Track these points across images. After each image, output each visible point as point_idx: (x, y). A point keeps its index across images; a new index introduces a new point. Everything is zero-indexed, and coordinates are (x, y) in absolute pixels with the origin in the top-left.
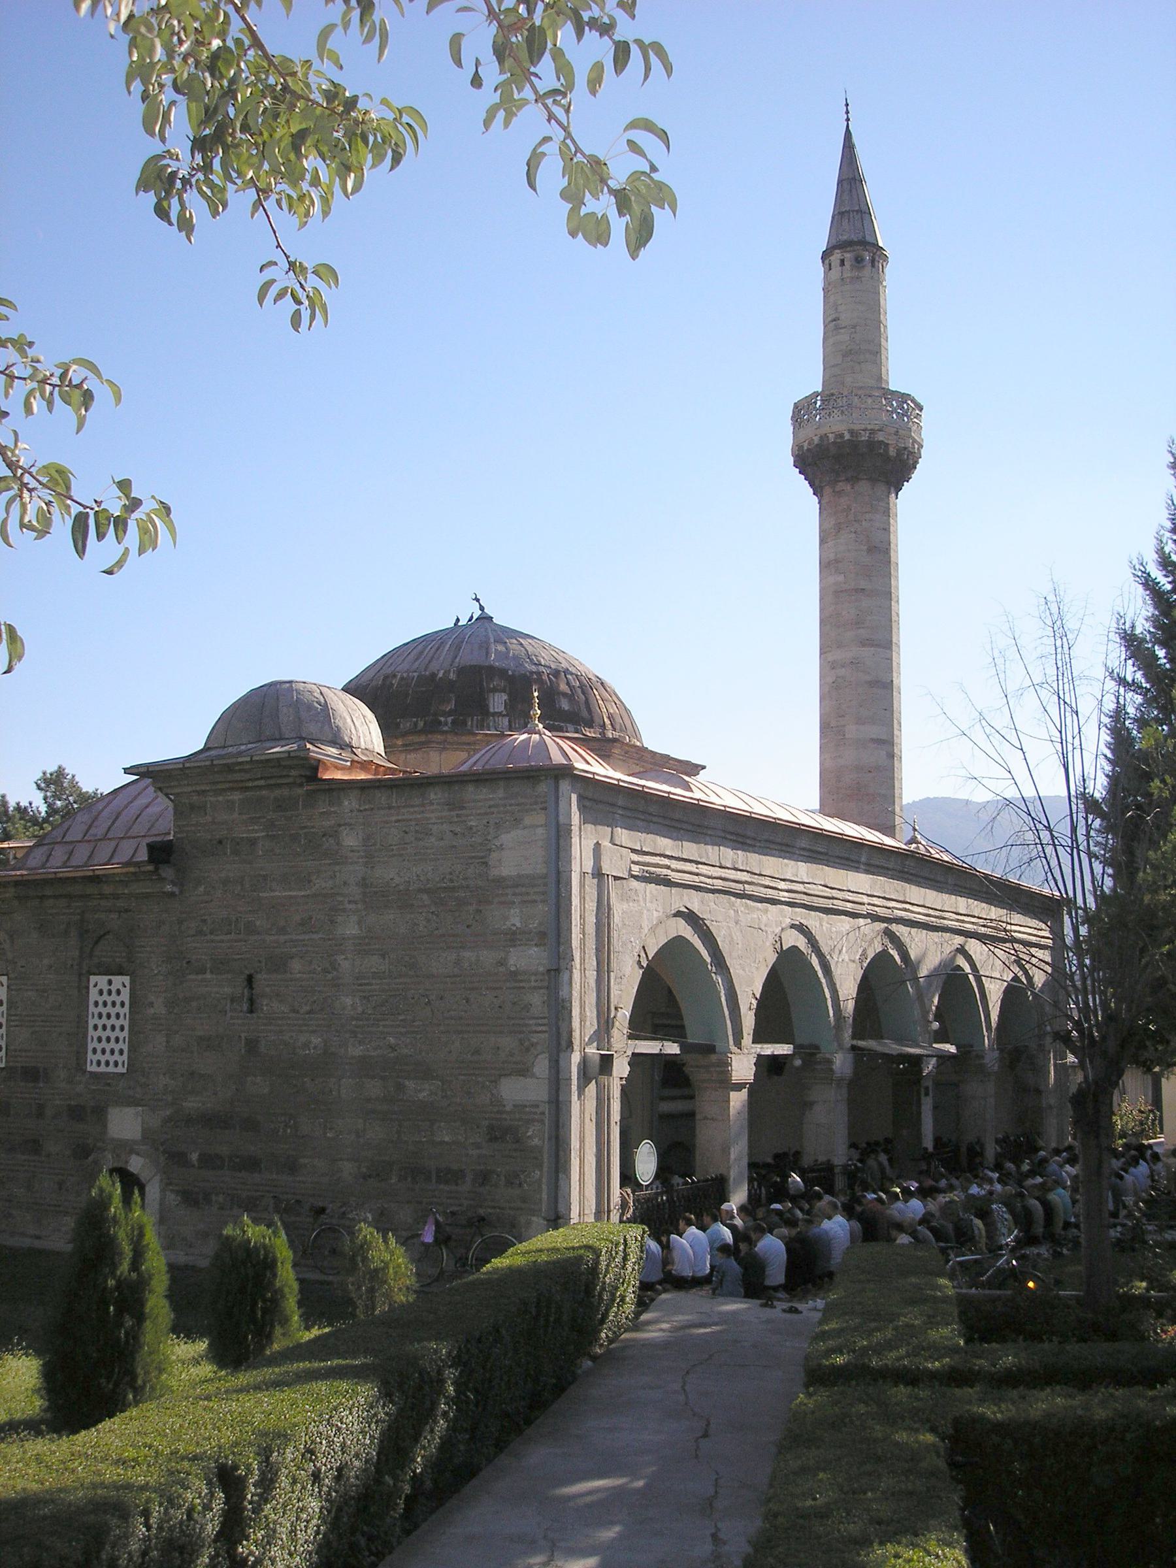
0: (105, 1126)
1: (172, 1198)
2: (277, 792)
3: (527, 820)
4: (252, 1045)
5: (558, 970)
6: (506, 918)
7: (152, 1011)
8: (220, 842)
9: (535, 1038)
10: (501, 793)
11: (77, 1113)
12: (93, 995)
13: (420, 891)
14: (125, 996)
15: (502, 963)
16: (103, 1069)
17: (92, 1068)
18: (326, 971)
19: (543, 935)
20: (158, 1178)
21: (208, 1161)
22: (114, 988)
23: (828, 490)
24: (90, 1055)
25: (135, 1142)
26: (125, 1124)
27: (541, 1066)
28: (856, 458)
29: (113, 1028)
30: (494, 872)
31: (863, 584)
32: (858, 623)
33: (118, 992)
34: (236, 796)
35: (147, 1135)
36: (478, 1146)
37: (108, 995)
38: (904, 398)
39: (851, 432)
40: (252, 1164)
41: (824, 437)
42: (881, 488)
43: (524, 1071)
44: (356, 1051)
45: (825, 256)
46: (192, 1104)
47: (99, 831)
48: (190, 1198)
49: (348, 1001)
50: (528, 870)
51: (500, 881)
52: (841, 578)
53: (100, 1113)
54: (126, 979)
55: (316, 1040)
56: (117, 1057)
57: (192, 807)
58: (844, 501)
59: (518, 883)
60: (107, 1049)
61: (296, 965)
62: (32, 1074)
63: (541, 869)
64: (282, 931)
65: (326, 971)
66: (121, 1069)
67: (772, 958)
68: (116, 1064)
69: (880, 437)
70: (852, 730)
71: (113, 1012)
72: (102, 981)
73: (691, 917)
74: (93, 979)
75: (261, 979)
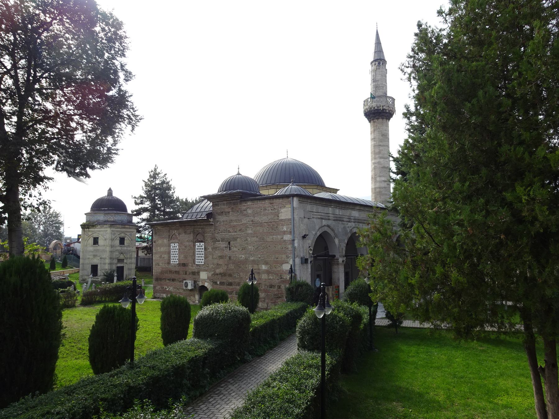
2: (234, 201)
4: (230, 258)
5: (294, 240)
10: (281, 200)
11: (194, 273)
12: (197, 247)
14: (203, 247)
17: (197, 263)
19: (291, 232)
21: (222, 283)
23: (372, 121)
26: (203, 275)
27: (291, 262)
28: (379, 113)
30: (280, 218)
31: (381, 144)
32: (379, 153)
34: (225, 202)
36: (278, 279)
37: (200, 247)
38: (390, 97)
39: (378, 107)
40: (230, 284)
41: (371, 108)
42: (385, 120)
44: (252, 259)
45: (372, 63)
46: (218, 271)
47: (198, 210)
50: (287, 217)
53: (198, 273)
55: (243, 256)
57: (216, 205)
58: (376, 124)
60: (200, 259)
61: (238, 240)
62: (184, 265)
63: (290, 217)
64: (236, 232)
67: (349, 235)
69: (384, 108)
70: (378, 179)
72: (198, 244)
73: (328, 226)
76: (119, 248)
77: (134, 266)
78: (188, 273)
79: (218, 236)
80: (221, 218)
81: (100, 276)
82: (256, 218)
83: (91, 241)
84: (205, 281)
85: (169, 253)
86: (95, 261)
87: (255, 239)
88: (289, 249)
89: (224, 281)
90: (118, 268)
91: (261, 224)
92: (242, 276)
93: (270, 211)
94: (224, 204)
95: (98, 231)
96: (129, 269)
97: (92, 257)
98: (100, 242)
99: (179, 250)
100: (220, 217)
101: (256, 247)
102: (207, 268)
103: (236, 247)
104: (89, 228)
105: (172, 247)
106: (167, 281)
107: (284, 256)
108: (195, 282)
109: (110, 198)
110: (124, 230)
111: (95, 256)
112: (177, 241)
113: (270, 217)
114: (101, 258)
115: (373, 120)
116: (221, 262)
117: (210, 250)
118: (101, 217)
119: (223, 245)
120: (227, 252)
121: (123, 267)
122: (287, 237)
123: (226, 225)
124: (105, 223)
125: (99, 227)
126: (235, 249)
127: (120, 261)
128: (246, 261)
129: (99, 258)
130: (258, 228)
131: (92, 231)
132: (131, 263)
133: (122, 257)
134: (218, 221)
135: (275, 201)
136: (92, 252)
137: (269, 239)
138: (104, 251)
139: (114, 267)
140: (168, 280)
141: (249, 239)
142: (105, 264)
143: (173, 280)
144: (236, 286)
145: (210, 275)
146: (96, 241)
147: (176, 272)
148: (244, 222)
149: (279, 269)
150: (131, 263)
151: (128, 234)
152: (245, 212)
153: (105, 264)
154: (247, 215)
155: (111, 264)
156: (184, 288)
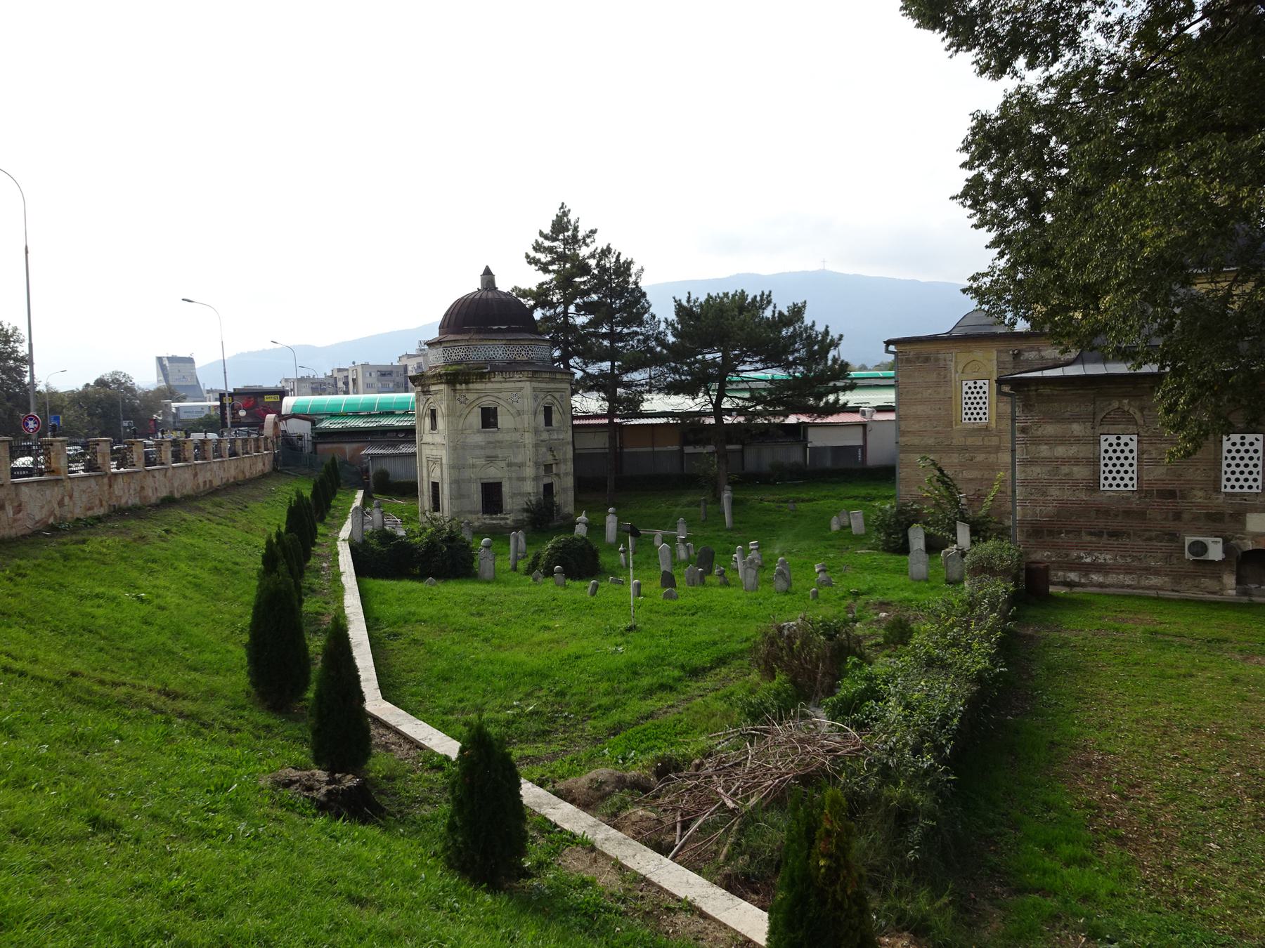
12: (1226, 445)
16: (1237, 490)
17: (1229, 490)
24: (1224, 482)
53: (1238, 517)
54: (1260, 436)
62: (1171, 494)
66: (1254, 490)
76: (545, 436)
77: (569, 482)
78: (1186, 516)
81: (511, 512)
83: (476, 419)
85: (1094, 462)
86: (493, 473)
90: (545, 486)
95: (495, 391)
96: (565, 490)
97: (482, 461)
98: (504, 420)
99: (1141, 452)
104: (467, 383)
105: (1104, 446)
108: (1226, 541)
109: (490, 295)
110: (552, 386)
111: (491, 459)
112: (1132, 428)
114: (509, 465)
118: (497, 351)
121: (551, 485)
124: (510, 368)
125: (498, 378)
127: (548, 468)
129: (503, 464)
131: (477, 391)
132: (566, 474)
133: (550, 459)
136: (482, 448)
138: (517, 445)
139: (542, 489)
140: (1091, 534)
142: (522, 479)
143: (1114, 534)
146: (489, 418)
147: (1128, 513)
150: (566, 474)
151: (557, 395)
153: (522, 479)
155: (536, 478)
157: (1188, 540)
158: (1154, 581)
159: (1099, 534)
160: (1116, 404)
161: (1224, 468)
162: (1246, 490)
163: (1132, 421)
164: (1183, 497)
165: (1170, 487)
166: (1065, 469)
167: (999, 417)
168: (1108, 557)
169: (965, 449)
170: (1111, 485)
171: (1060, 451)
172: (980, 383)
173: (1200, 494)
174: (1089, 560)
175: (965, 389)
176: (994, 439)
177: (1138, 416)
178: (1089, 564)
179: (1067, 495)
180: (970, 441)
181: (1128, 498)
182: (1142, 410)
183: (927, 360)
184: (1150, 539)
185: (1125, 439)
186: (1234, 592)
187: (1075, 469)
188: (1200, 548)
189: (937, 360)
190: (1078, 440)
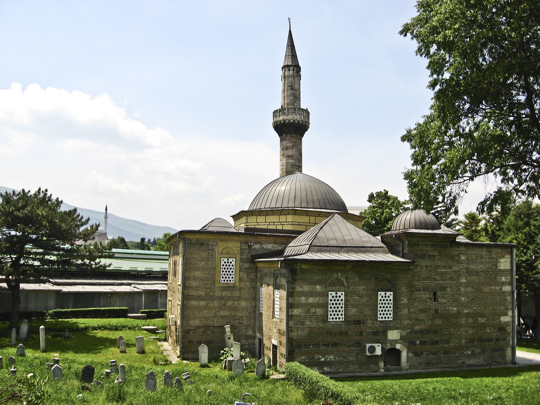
0: (387, 336)
1: (410, 355)
3: (506, 256)
4: (436, 311)
6: (501, 279)
7: (402, 302)
8: (424, 255)
9: (509, 307)
10: (500, 250)
12: (380, 297)
13: (481, 272)
14: (391, 297)
15: (501, 289)
16: (384, 319)
17: (380, 319)
18: (457, 291)
20: (406, 350)
22: (387, 295)
25: (398, 340)
26: (393, 335)
27: (510, 313)
29: (384, 307)
33: (389, 297)
34: (429, 243)
35: (402, 338)
37: (385, 298)
40: (437, 342)
41: (294, 121)
43: (506, 314)
44: (466, 311)
46: (417, 328)
48: (416, 354)
49: (463, 299)
51: (500, 270)
52: (293, 161)
53: (385, 333)
54: (392, 293)
55: (455, 309)
56: (388, 315)
59: (504, 271)
61: (448, 289)
62: (358, 322)
64: (444, 280)
65: (457, 291)
66: (390, 319)
68: (388, 318)
71: (387, 302)
72: (383, 293)
74: (379, 293)
75: (439, 293)
79: (419, 284)
80: (424, 263)
82: (471, 266)
84: (396, 342)
85: (325, 306)
87: (470, 289)
88: (508, 301)
89: (426, 339)
91: (477, 273)
92: (452, 332)
93: (488, 260)
94: (427, 245)
99: (346, 301)
100: (421, 260)
101: (470, 298)
102: (398, 326)
103: (444, 298)
105: (330, 297)
106: (323, 348)
107: (502, 308)
113: (487, 266)
115: (290, 134)
116: (422, 316)
117: (405, 301)
119: (425, 295)
120: (432, 305)
122: (507, 288)
123: (431, 271)
126: (443, 300)
128: (458, 315)
130: (474, 277)
134: (418, 266)
135: (493, 249)
137: (487, 289)
140: (324, 345)
141: (462, 289)
143: (335, 345)
144: (444, 344)
145: (404, 333)
147: (341, 333)
148: (455, 268)
149: (497, 321)
152: (457, 258)
154: (459, 262)
156: (368, 354)
157: (368, 345)
158: (352, 368)
159: (327, 345)
160: (335, 275)
161: (379, 309)
162: (387, 319)
163: (342, 285)
164: (364, 324)
165: (358, 319)
166: (313, 310)
167: (241, 280)
168: (332, 357)
169: (221, 298)
170: (333, 318)
171: (311, 300)
172: (230, 260)
173: (370, 322)
174: (323, 360)
175: (222, 263)
176: (237, 292)
177: (345, 282)
178: (323, 362)
179: (314, 324)
180: (224, 293)
181: (341, 325)
182: (346, 279)
183: (202, 244)
184: (350, 346)
185: (339, 293)
186: (382, 370)
187: (318, 310)
188: (372, 349)
189: (208, 245)
190: (319, 294)
